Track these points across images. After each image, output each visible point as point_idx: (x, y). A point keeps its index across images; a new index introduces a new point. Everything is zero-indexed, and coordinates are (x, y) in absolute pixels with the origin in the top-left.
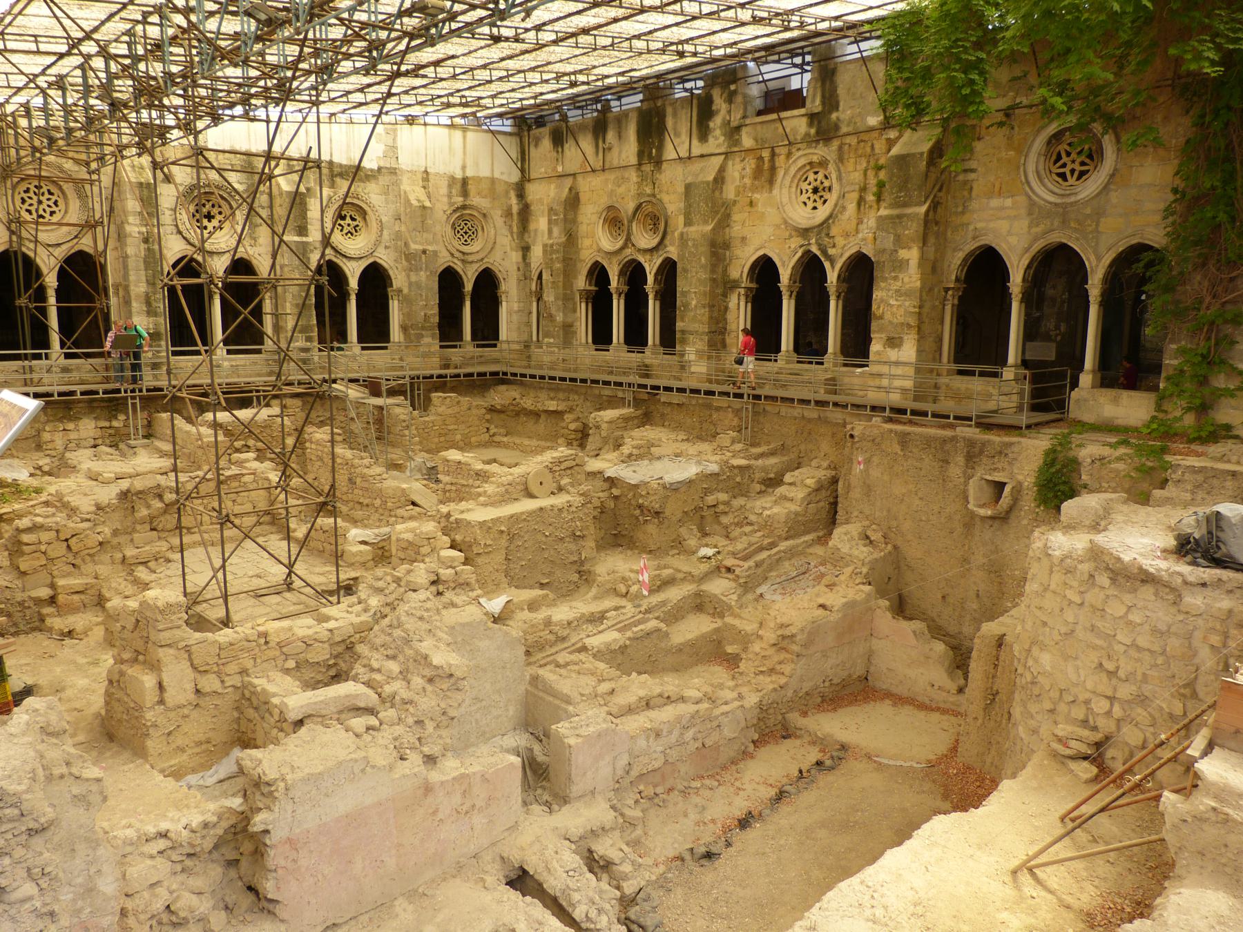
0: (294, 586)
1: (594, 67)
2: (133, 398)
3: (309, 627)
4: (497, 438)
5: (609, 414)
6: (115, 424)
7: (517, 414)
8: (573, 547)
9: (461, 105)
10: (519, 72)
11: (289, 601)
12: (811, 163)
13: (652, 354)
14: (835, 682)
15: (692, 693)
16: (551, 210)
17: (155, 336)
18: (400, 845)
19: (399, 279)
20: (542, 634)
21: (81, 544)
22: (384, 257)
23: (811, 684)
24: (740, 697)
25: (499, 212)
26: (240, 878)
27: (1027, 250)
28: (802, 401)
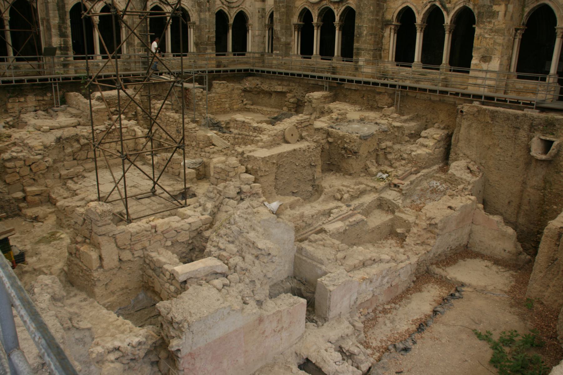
2: (55, 84)
3: (178, 222)
4: (248, 106)
5: (317, 94)
6: (46, 98)
7: (259, 93)
8: (310, 171)
11: (154, 203)
13: (337, 61)
14: (453, 247)
15: (385, 257)
17: (64, 49)
18: (246, 351)
19: (194, 17)
20: (299, 222)
21: (37, 168)
22: (186, 4)
23: (442, 249)
24: (409, 258)
26: (160, 371)
28: (431, 91)
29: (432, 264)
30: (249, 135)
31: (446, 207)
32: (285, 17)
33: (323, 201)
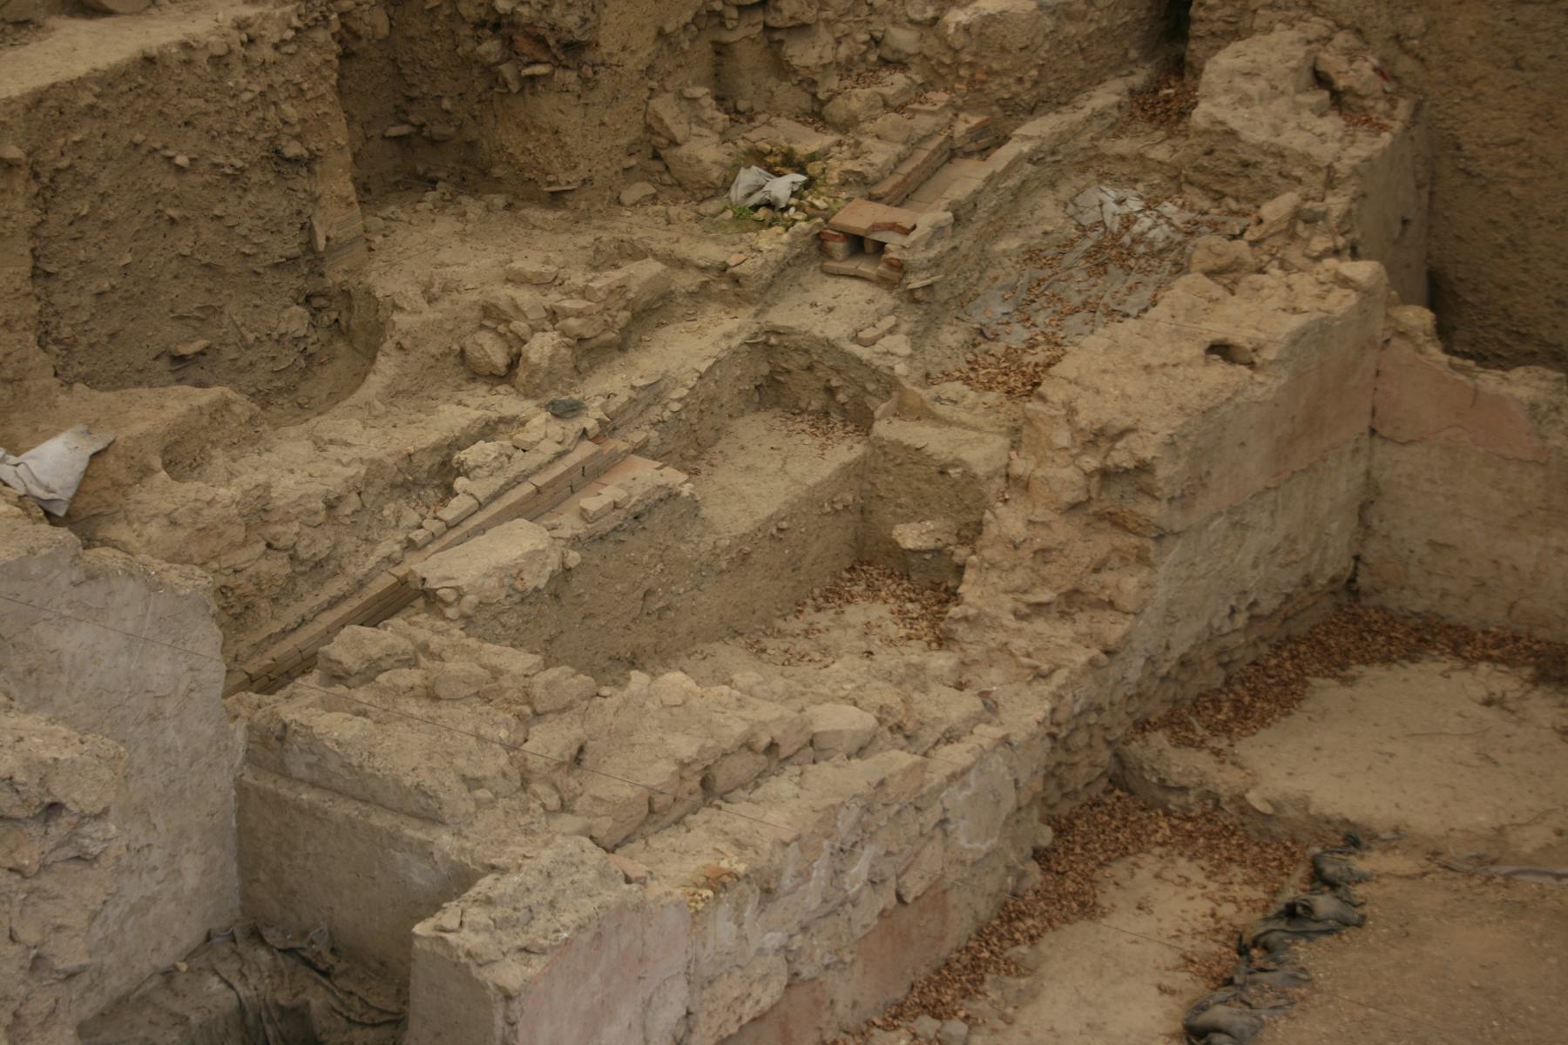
8: (276, 203)
14: (1268, 604)
20: (240, 557)
23: (1198, 626)
24: (991, 706)
29: (1143, 726)
31: (1192, 351)
33: (394, 394)
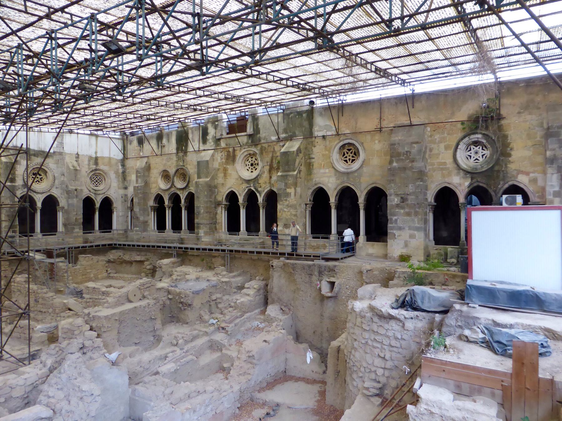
0: (4, 357)
1: (158, 113)
4: (112, 275)
5: (166, 261)
9: (96, 126)
10: (124, 114)
12: (250, 154)
13: (184, 232)
14: (272, 375)
16: (137, 172)
19: (63, 202)
24: (231, 387)
25: (113, 172)
27: (336, 189)
28: (251, 252)
30: (99, 299)
32: (142, 201)
